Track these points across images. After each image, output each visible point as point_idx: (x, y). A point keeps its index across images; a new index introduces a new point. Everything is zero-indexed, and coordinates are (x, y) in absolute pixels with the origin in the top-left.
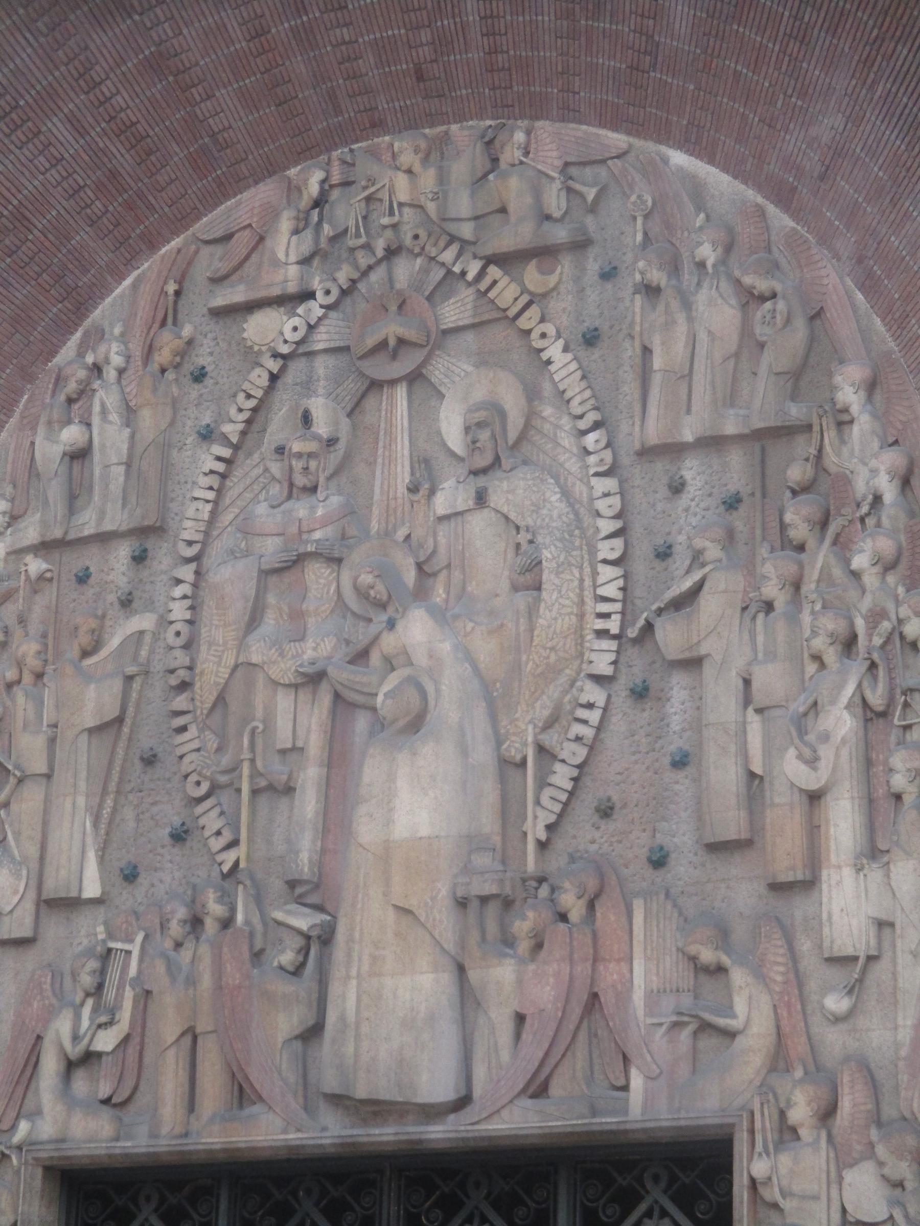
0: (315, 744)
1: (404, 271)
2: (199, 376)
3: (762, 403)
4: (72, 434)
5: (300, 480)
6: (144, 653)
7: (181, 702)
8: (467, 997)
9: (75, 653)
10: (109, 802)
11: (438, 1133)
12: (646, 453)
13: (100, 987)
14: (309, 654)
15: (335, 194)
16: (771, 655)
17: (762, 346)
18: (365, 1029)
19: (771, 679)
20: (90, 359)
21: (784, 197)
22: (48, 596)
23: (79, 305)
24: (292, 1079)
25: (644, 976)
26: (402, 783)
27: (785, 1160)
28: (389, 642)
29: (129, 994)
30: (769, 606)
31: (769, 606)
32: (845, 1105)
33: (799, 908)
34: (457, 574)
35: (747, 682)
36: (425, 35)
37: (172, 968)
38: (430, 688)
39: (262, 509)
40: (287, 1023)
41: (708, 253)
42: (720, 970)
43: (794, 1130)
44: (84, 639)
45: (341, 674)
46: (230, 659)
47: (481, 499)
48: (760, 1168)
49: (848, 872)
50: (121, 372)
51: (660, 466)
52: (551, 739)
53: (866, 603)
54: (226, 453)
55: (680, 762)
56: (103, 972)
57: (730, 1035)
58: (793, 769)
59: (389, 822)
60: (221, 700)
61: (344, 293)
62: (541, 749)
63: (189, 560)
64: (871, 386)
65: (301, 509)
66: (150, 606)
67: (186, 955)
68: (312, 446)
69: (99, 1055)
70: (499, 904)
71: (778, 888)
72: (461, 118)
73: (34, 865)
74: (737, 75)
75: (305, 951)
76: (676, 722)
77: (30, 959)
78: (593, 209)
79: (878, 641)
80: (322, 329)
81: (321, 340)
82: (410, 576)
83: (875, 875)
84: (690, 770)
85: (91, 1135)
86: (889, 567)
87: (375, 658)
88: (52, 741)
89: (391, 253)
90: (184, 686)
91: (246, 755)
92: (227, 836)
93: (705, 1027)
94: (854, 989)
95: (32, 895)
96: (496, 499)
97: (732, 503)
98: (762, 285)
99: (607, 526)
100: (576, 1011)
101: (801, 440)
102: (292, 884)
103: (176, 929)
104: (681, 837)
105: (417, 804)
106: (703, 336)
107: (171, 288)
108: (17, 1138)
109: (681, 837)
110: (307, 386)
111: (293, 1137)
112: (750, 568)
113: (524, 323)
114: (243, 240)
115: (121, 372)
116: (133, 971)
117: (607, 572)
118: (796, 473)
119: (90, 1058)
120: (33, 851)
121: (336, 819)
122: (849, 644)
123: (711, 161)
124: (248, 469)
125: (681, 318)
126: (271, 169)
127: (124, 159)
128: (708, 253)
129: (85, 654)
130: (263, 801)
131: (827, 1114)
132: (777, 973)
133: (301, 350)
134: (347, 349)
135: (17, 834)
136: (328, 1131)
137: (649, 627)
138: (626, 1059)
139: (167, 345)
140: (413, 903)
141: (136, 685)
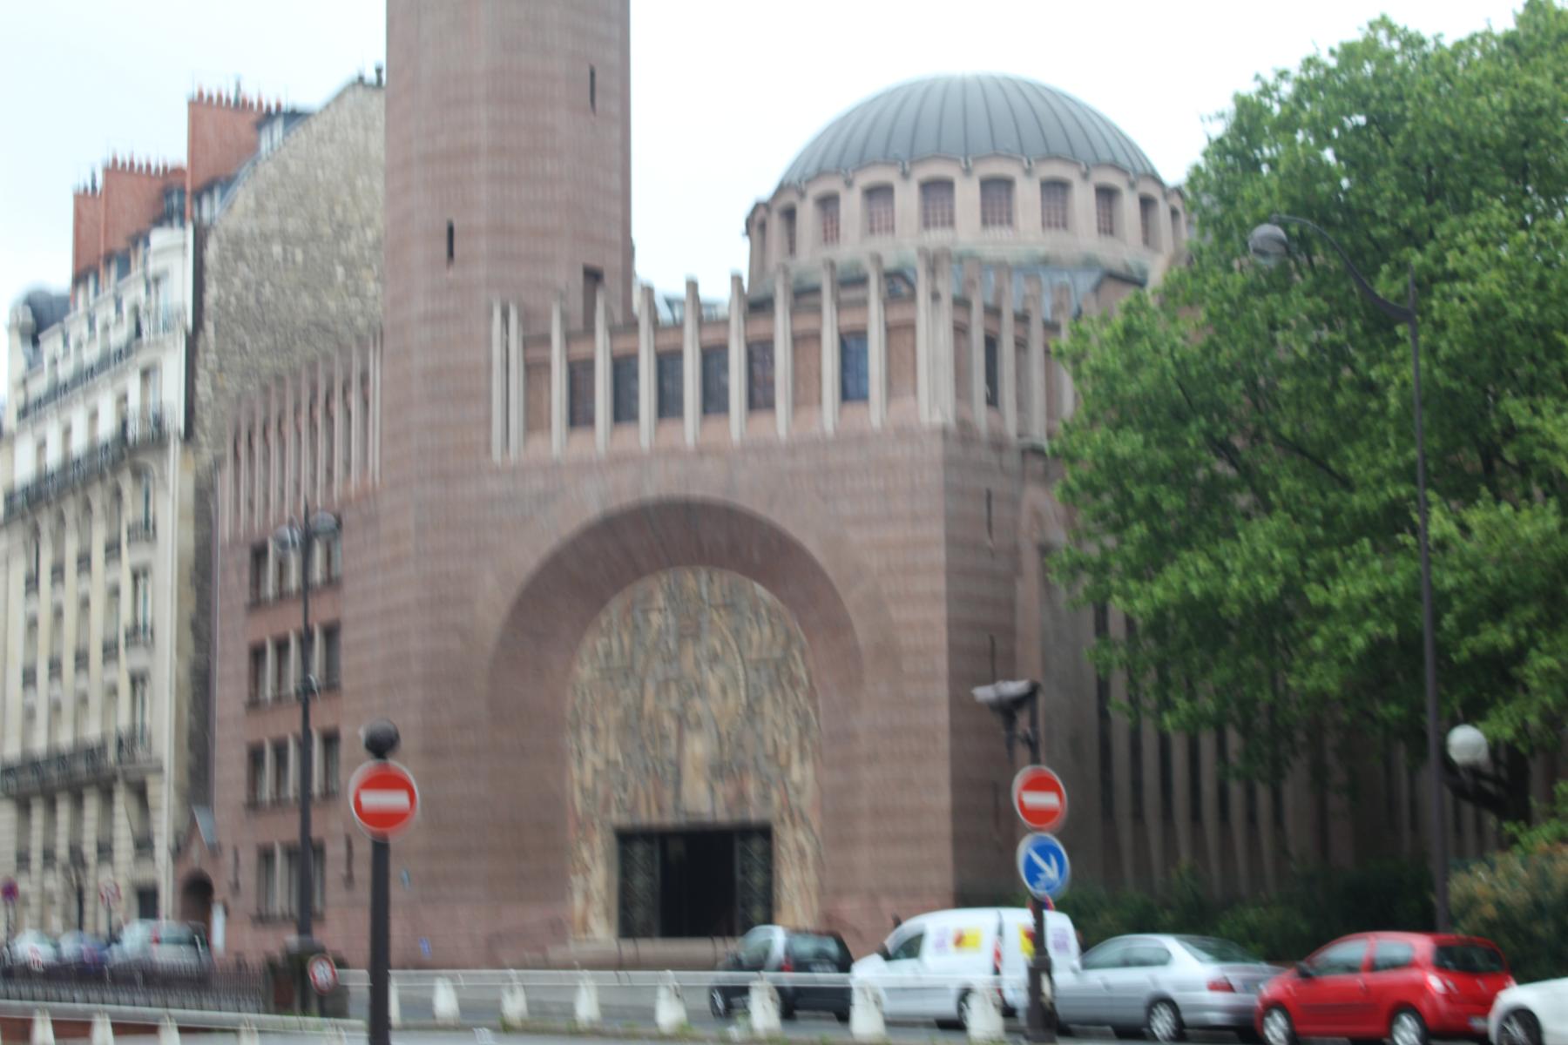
3: (777, 653)
8: (712, 790)
19: (780, 720)
70: (719, 770)
105: (698, 748)
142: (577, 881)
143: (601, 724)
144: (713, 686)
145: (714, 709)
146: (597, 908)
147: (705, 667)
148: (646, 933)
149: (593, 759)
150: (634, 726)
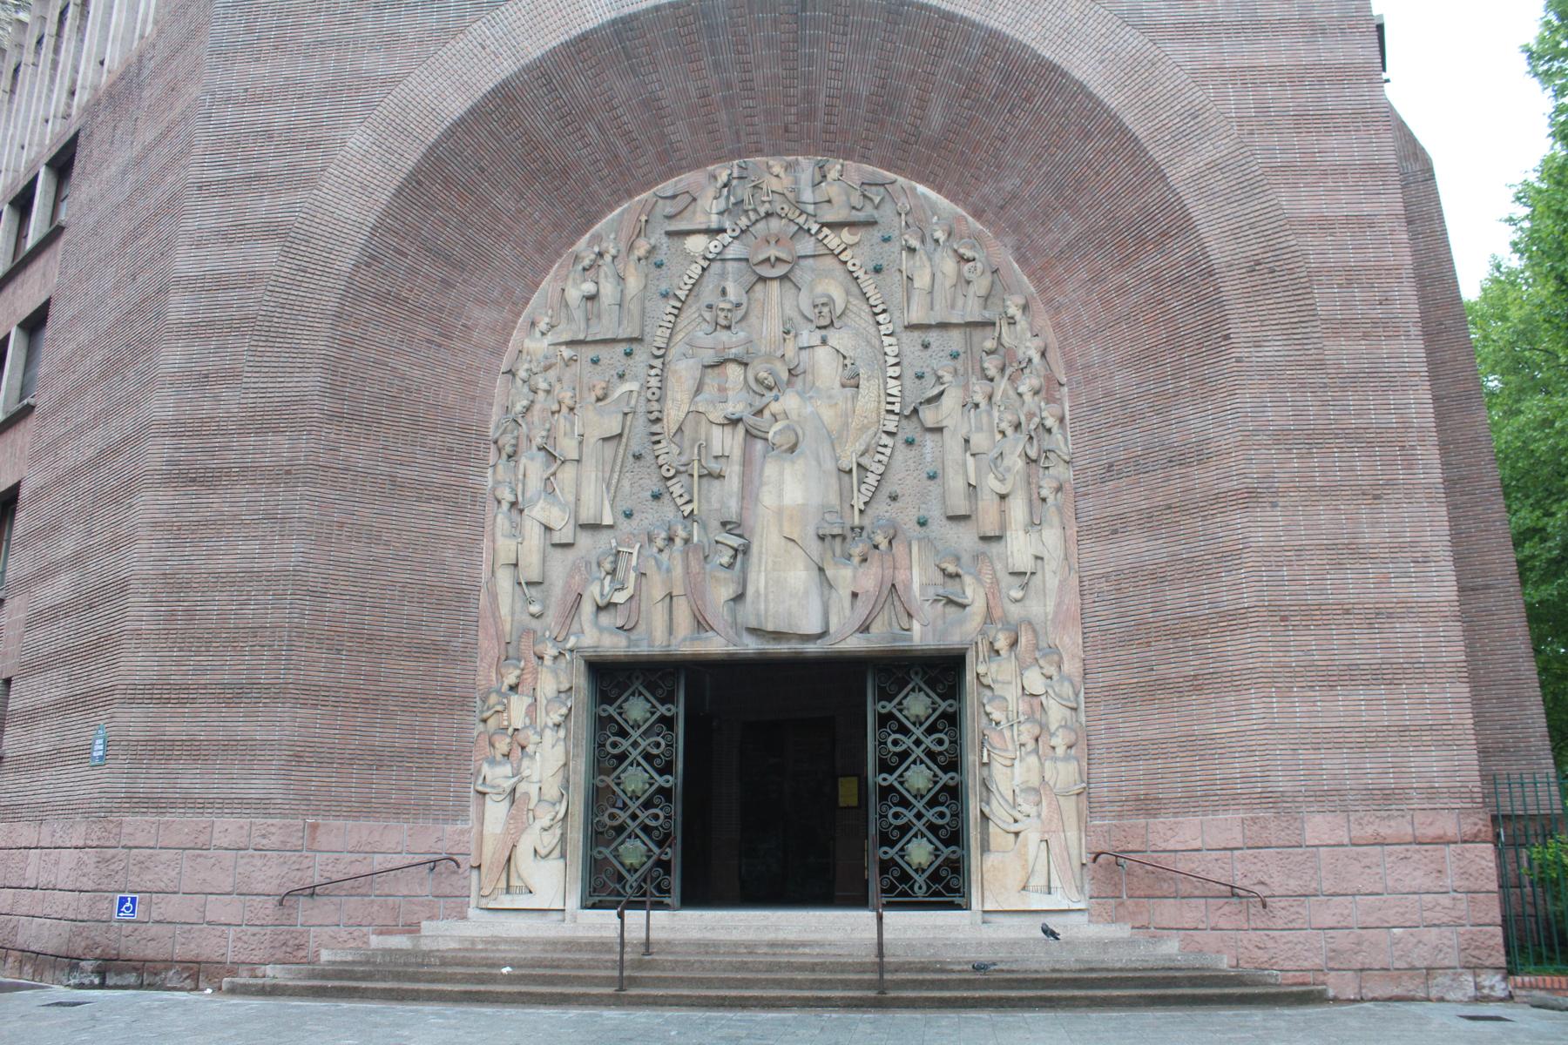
0: (737, 454)
1: (774, 224)
2: (659, 265)
3: (974, 312)
4: (589, 287)
5: (724, 323)
6: (633, 402)
7: (656, 428)
8: (826, 583)
9: (593, 398)
10: (616, 476)
11: (812, 648)
12: (911, 327)
13: (615, 570)
14: (731, 410)
15: (735, 182)
16: (979, 429)
17: (968, 282)
18: (771, 596)
19: (979, 441)
20: (596, 249)
21: (978, 214)
22: (575, 368)
23: (590, 223)
24: (730, 620)
25: (918, 578)
26: (788, 476)
27: (994, 666)
28: (775, 407)
29: (632, 575)
30: (977, 406)
31: (977, 406)
32: (1023, 640)
33: (994, 548)
34: (809, 377)
35: (967, 441)
36: (793, 110)
37: (658, 564)
38: (800, 432)
39: (701, 334)
40: (725, 592)
41: (940, 235)
42: (958, 575)
43: (997, 652)
44: (600, 393)
45: (751, 420)
46: (685, 408)
47: (824, 342)
48: (982, 669)
49: (1021, 533)
50: (614, 258)
51: (916, 334)
52: (865, 461)
53: (1025, 409)
54: (678, 305)
55: (932, 477)
56: (615, 562)
57: (964, 606)
58: (992, 483)
59: (780, 496)
60: (680, 429)
61: (742, 231)
62: (859, 465)
63: (658, 357)
64: (1025, 308)
65: (724, 336)
66: (635, 378)
67: (664, 556)
68: (728, 306)
69: (615, 605)
70: (838, 538)
71: (985, 539)
72: (806, 153)
73: (572, 506)
74: (962, 153)
75: (735, 557)
76: (929, 458)
77: (570, 555)
78: (877, 207)
79: (1032, 427)
80: (731, 248)
81: (731, 253)
82: (785, 376)
83: (1035, 536)
84: (938, 481)
85: (614, 645)
86: (1036, 393)
87: (767, 413)
88: (581, 443)
89: (768, 215)
90: (658, 420)
91: (696, 457)
92: (686, 498)
93: (950, 602)
94: (1024, 587)
95: (572, 521)
96: (831, 342)
97: (955, 356)
98: (969, 254)
99: (892, 361)
100: (885, 592)
101: (988, 330)
102: (724, 524)
103: (660, 543)
104: (935, 514)
106: (939, 275)
107: (644, 218)
108: (569, 645)
109: (935, 514)
110: (723, 275)
111: (732, 649)
112: (966, 387)
113: (842, 257)
114: (687, 199)
115: (614, 258)
116: (634, 563)
117: (892, 382)
118: (990, 344)
119: (610, 605)
120: (572, 499)
121: (748, 491)
122: (1018, 426)
123: (939, 192)
124: (690, 313)
125: (927, 264)
126: (697, 165)
127: (623, 151)
128: (940, 235)
129: (599, 400)
130: (704, 480)
131: (1014, 644)
132: (987, 579)
133: (720, 258)
134: (747, 260)
135: (562, 490)
136: (751, 646)
137: (915, 411)
138: (910, 616)
139: (642, 247)
140: (794, 537)
141: (629, 417)
142: (498, 775)
143: (568, 447)
144: (825, 365)
145: (828, 415)
146: (539, 836)
147: (808, 336)
148: (649, 896)
149: (540, 511)
150: (643, 444)
